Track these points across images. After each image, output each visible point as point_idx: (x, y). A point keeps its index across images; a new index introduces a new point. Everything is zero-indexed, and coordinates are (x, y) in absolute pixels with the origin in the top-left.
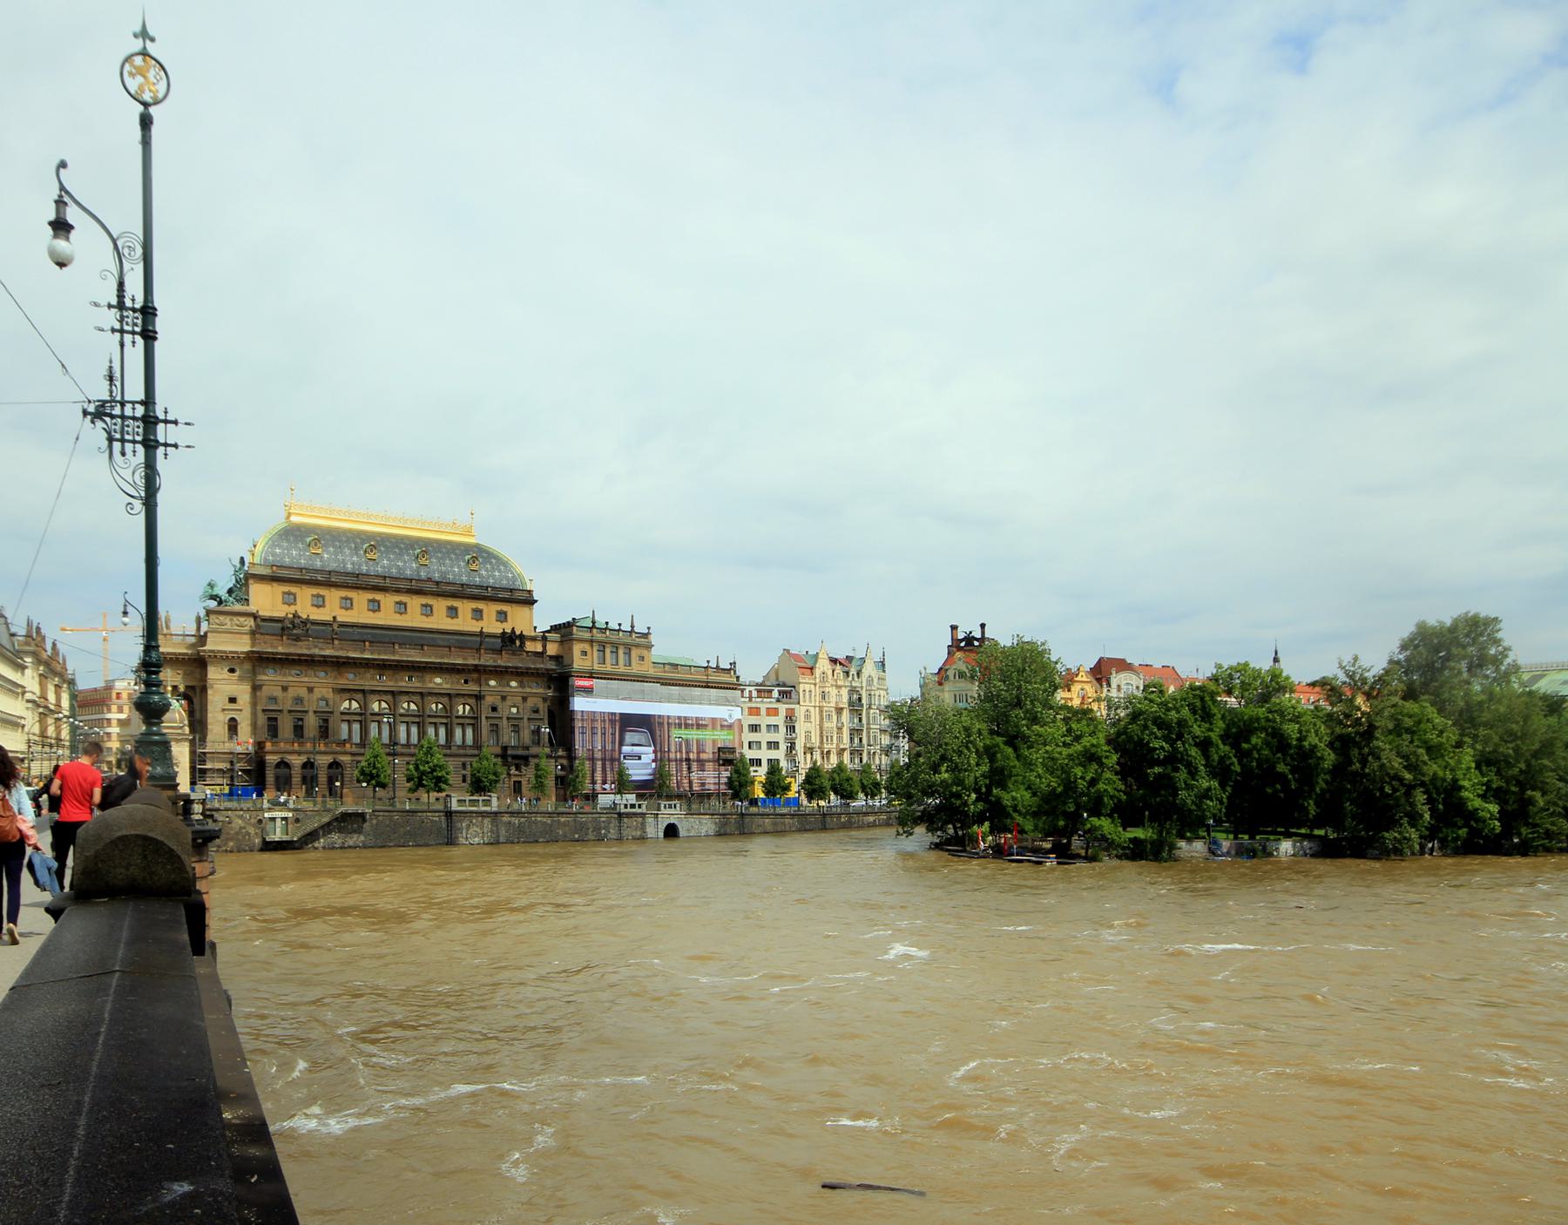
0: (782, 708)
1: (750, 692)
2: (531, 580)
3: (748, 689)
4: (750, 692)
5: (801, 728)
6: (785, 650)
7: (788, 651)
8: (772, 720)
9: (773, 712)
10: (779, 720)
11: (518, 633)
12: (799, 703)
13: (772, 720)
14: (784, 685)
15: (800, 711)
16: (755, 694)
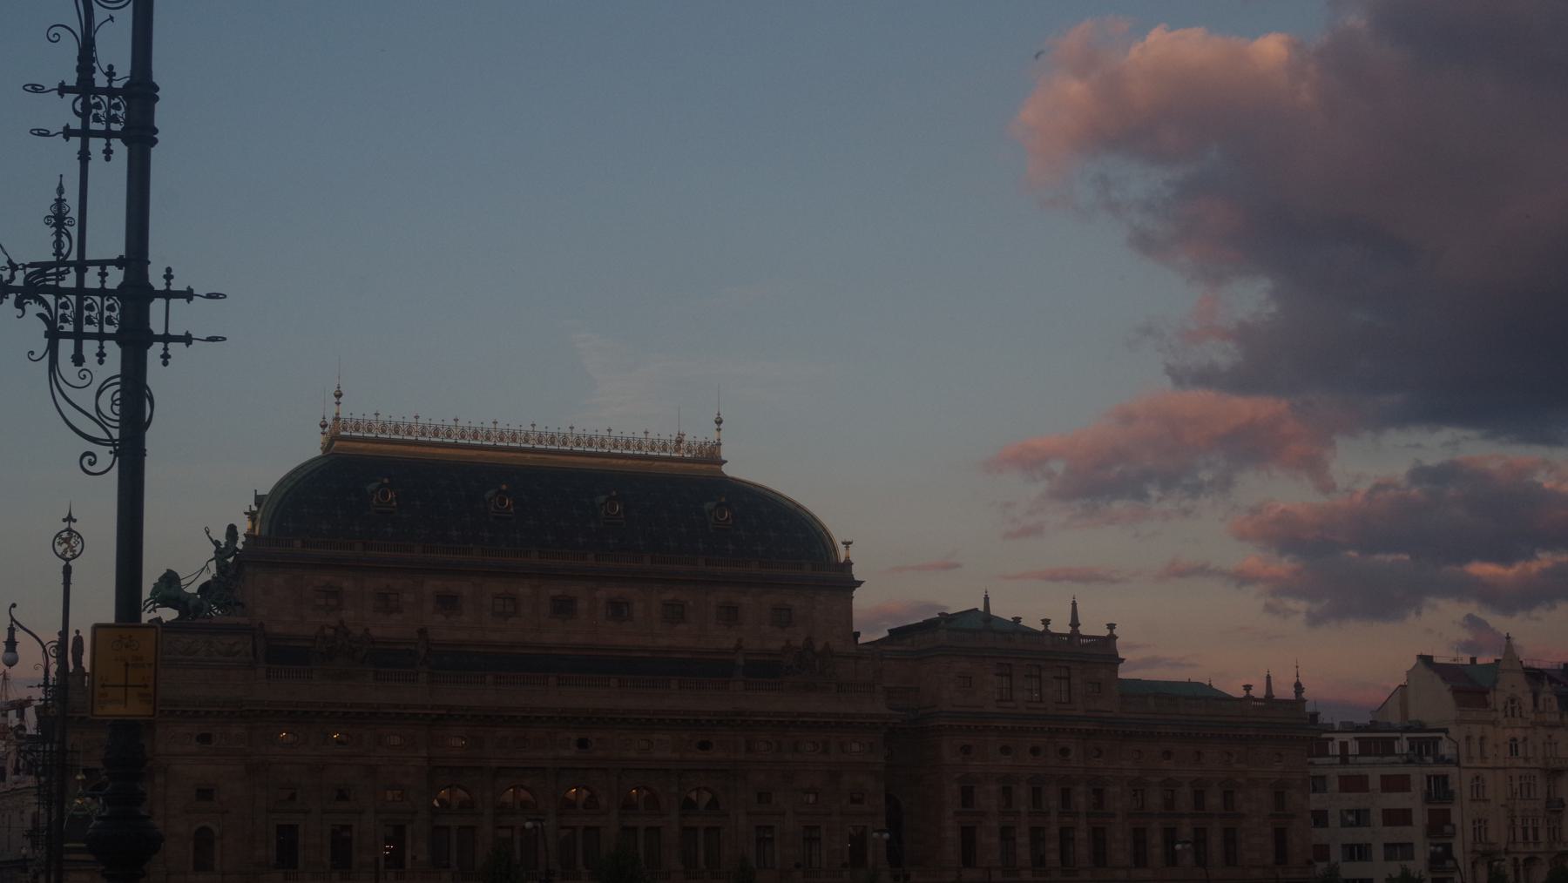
0: (1418, 775)
1: (1344, 745)
2: (847, 544)
3: (1339, 738)
4: (1344, 745)
5: (1461, 815)
6: (1421, 657)
7: (1426, 660)
8: (1396, 800)
9: (1395, 784)
10: (1412, 800)
11: (819, 646)
12: (1458, 764)
13: (1396, 800)
14: (1422, 728)
15: (1460, 781)
16: (1353, 748)
